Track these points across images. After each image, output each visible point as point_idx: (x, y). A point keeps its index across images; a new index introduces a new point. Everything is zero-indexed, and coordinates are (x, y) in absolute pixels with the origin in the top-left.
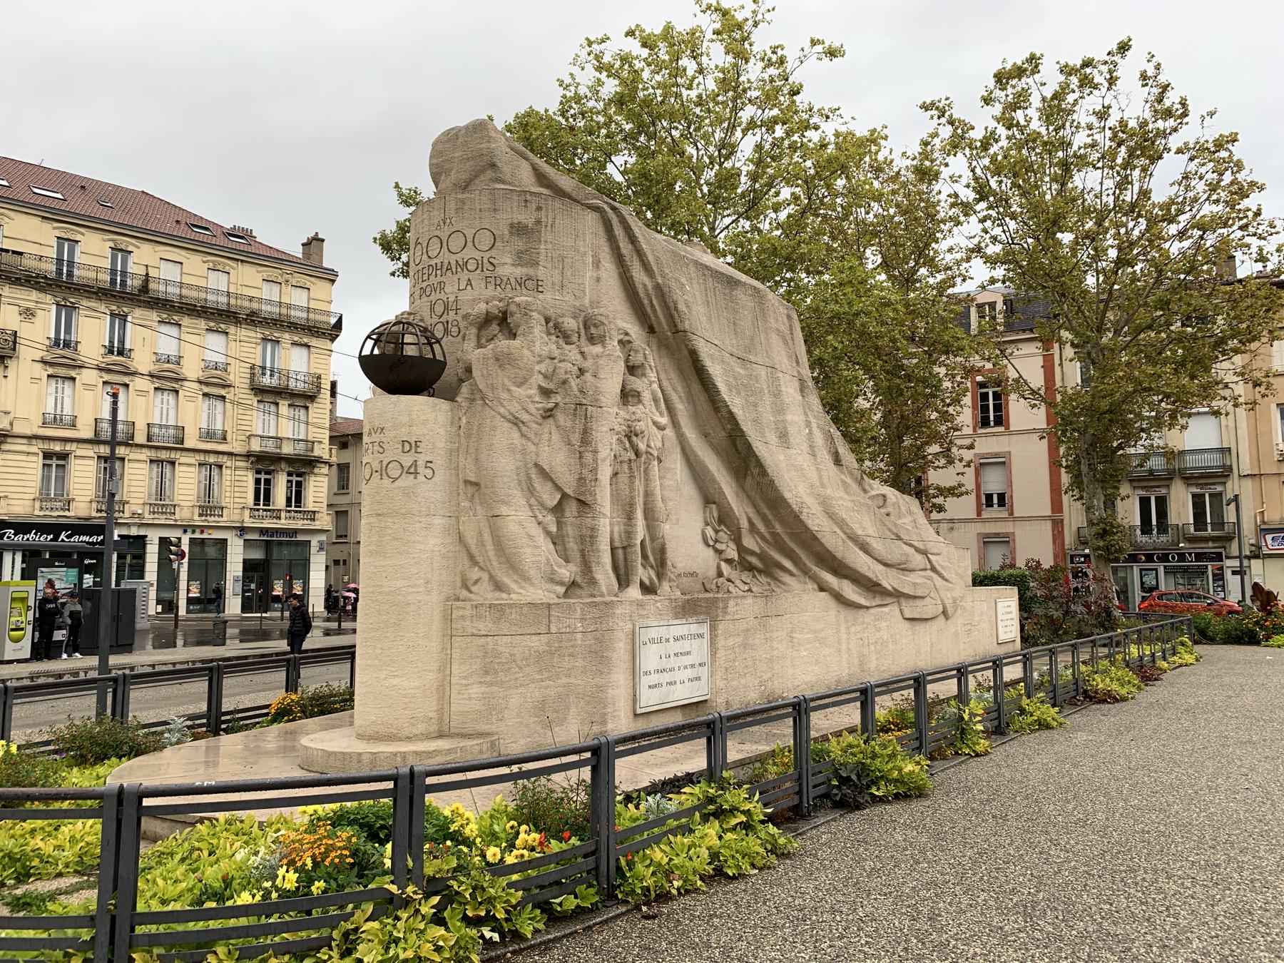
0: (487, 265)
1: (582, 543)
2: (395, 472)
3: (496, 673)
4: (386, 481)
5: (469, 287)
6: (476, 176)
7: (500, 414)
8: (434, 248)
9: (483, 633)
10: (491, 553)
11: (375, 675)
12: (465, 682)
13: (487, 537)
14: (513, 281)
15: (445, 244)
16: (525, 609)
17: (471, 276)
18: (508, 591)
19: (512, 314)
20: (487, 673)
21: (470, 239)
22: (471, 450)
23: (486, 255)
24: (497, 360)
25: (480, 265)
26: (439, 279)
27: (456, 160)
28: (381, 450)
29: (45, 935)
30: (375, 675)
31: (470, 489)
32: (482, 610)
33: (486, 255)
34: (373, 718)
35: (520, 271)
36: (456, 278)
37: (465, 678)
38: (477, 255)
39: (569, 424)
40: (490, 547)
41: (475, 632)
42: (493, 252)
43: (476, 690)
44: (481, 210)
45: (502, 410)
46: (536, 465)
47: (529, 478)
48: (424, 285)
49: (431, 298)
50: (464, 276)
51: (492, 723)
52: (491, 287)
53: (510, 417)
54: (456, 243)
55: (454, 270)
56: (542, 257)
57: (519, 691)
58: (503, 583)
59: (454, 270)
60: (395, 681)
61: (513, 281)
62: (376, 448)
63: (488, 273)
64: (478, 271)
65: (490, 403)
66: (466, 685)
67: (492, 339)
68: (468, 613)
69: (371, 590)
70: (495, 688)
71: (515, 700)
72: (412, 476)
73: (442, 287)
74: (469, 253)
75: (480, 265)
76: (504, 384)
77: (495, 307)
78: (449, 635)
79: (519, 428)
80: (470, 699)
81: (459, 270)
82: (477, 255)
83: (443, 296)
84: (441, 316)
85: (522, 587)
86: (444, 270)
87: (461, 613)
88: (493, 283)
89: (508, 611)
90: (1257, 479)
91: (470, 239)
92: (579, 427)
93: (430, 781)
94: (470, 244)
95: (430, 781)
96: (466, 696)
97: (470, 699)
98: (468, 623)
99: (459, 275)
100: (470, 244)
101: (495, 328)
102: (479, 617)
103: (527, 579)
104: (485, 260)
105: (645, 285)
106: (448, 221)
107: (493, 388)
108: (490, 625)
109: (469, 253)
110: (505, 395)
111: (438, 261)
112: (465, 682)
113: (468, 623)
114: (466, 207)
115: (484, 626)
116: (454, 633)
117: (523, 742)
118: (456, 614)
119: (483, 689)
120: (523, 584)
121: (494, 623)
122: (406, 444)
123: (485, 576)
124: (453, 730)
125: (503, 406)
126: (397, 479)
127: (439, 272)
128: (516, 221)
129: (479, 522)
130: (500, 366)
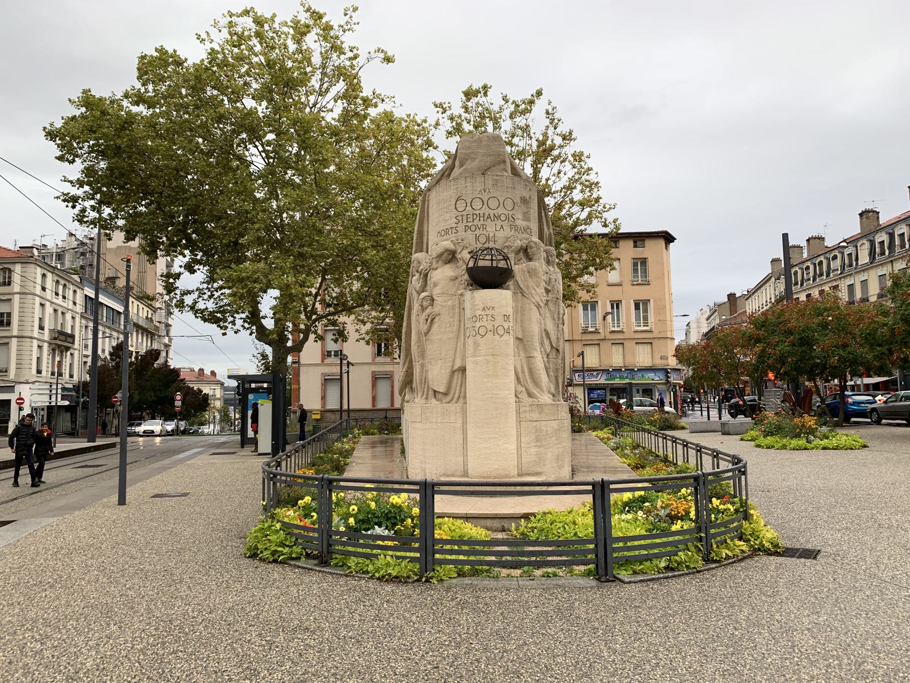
0: (511, 219)
2: (501, 332)
4: (497, 337)
6: (494, 166)
8: (477, 204)
10: (527, 377)
15: (485, 203)
17: (503, 223)
19: (531, 248)
21: (501, 203)
22: (519, 321)
23: (511, 213)
24: (529, 272)
25: (507, 218)
29: (654, 541)
31: (518, 342)
33: (511, 213)
34: (497, 467)
35: (525, 223)
36: (494, 223)
37: (528, 444)
39: (553, 309)
40: (527, 374)
42: (514, 212)
43: (533, 450)
46: (545, 330)
50: (499, 223)
52: (513, 231)
54: (493, 203)
58: (533, 393)
60: (507, 446)
62: (490, 318)
63: (512, 223)
64: (507, 221)
71: (549, 455)
73: (484, 227)
75: (507, 218)
77: (524, 243)
78: (519, 421)
80: (531, 455)
82: (506, 212)
83: (485, 232)
87: (524, 409)
90: (571, 342)
91: (501, 203)
92: (557, 310)
93: (612, 486)
94: (501, 205)
95: (612, 486)
97: (531, 455)
99: (495, 222)
100: (501, 205)
102: (533, 411)
103: (543, 391)
107: (528, 287)
109: (501, 211)
110: (534, 292)
115: (535, 416)
117: (553, 476)
118: (522, 409)
119: (536, 449)
123: (524, 390)
124: (523, 472)
127: (482, 219)
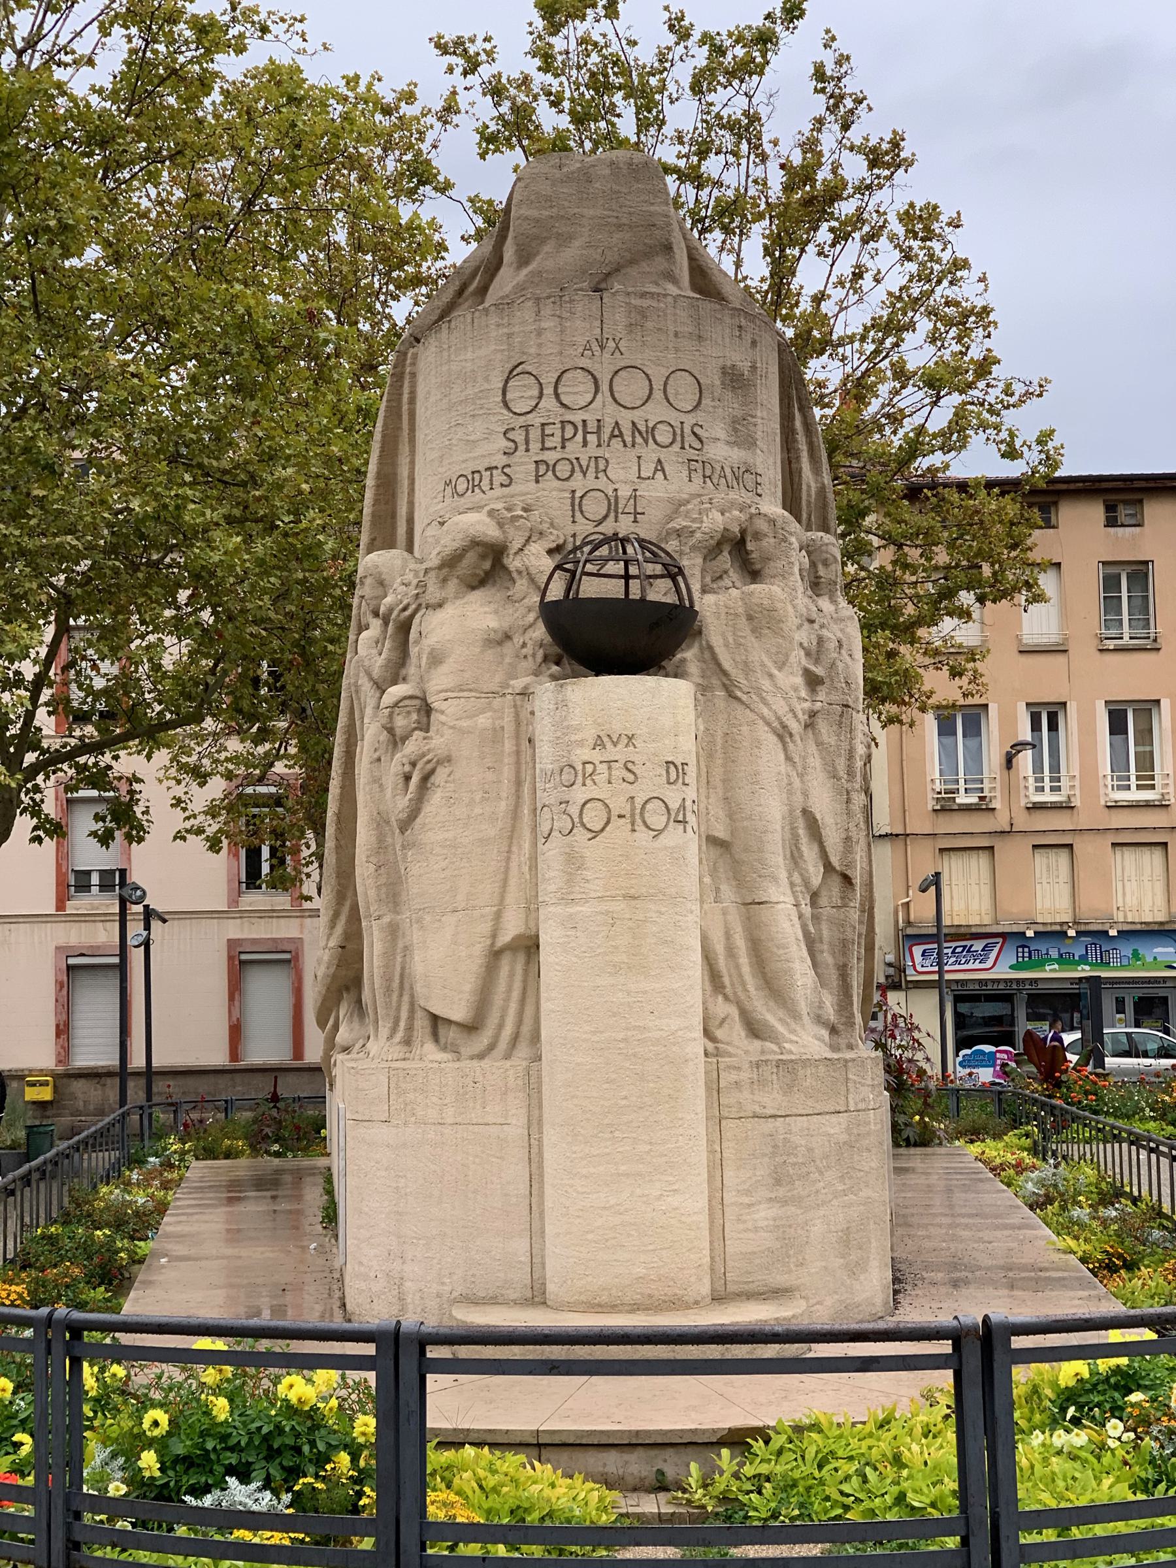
0: (690, 439)
1: (844, 954)
2: (657, 819)
3: (792, 1182)
4: (643, 835)
5: (659, 475)
6: (632, 262)
7: (763, 718)
8: (577, 391)
9: (769, 1112)
10: (746, 970)
11: (638, 1191)
12: (746, 1200)
13: (740, 943)
14: (728, 471)
15: (605, 387)
16: (822, 1069)
17: (663, 454)
18: (773, 1037)
19: (757, 536)
20: (778, 1182)
21: (658, 385)
22: (717, 780)
23: (689, 420)
24: (750, 618)
25: (678, 436)
26: (592, 450)
27: (585, 221)
28: (631, 777)
29: (1159, 1521)
30: (638, 1191)
31: (714, 852)
32: (767, 1071)
33: (689, 420)
34: (640, 1271)
35: (736, 455)
36: (632, 454)
37: (748, 1193)
38: (674, 417)
39: (832, 740)
40: (744, 960)
41: (758, 1110)
42: (699, 416)
43: (764, 1214)
44: (676, 335)
45: (765, 711)
46: (806, 812)
47: (795, 837)
48: (551, 457)
49: (572, 484)
50: (651, 453)
51: (790, 1271)
52: (698, 479)
53: (776, 724)
54: (631, 388)
55: (628, 439)
56: (759, 434)
57: (822, 1213)
58: (766, 1024)
59: (628, 439)
60: (674, 1201)
61: (728, 471)
62: (618, 772)
63: (693, 454)
64: (676, 447)
65: (744, 698)
66: (750, 1205)
67: (721, 577)
68: (745, 1076)
69: (621, 1036)
70: (791, 1210)
71: (817, 1229)
72: (681, 827)
73: (601, 466)
74: (656, 412)
75: (678, 436)
76: (763, 665)
77: (734, 520)
78: (717, 1119)
79: (784, 744)
80: (756, 1229)
81: (639, 440)
82: (674, 417)
83: (602, 483)
84: (600, 523)
85: (793, 1032)
86: (605, 436)
87: (733, 1076)
88: (700, 471)
89: (801, 1073)
90: (900, 842)
91: (658, 385)
92: (845, 746)
93: (1018, 1342)
94: (658, 394)
95: (1018, 1342)
96: (750, 1225)
97: (756, 1229)
98: (746, 1094)
99: (638, 450)
100: (658, 394)
101: (725, 559)
102: (762, 1083)
103: (795, 1015)
104: (687, 430)
105: (809, 487)
106: (611, 344)
107: (747, 668)
108: (779, 1097)
109: (656, 412)
110: (766, 684)
111: (591, 417)
112: (746, 1200)
113: (746, 1094)
114: (649, 325)
115: (772, 1100)
116: (725, 1113)
117: (829, 1302)
118: (727, 1078)
119: (775, 1211)
120: (793, 1025)
121: (785, 1094)
122: (672, 769)
123: (734, 1012)
124: (731, 1288)
125: (766, 704)
126: (661, 832)
127: (591, 438)
128: (729, 363)
129: (725, 913)
130: (753, 631)
